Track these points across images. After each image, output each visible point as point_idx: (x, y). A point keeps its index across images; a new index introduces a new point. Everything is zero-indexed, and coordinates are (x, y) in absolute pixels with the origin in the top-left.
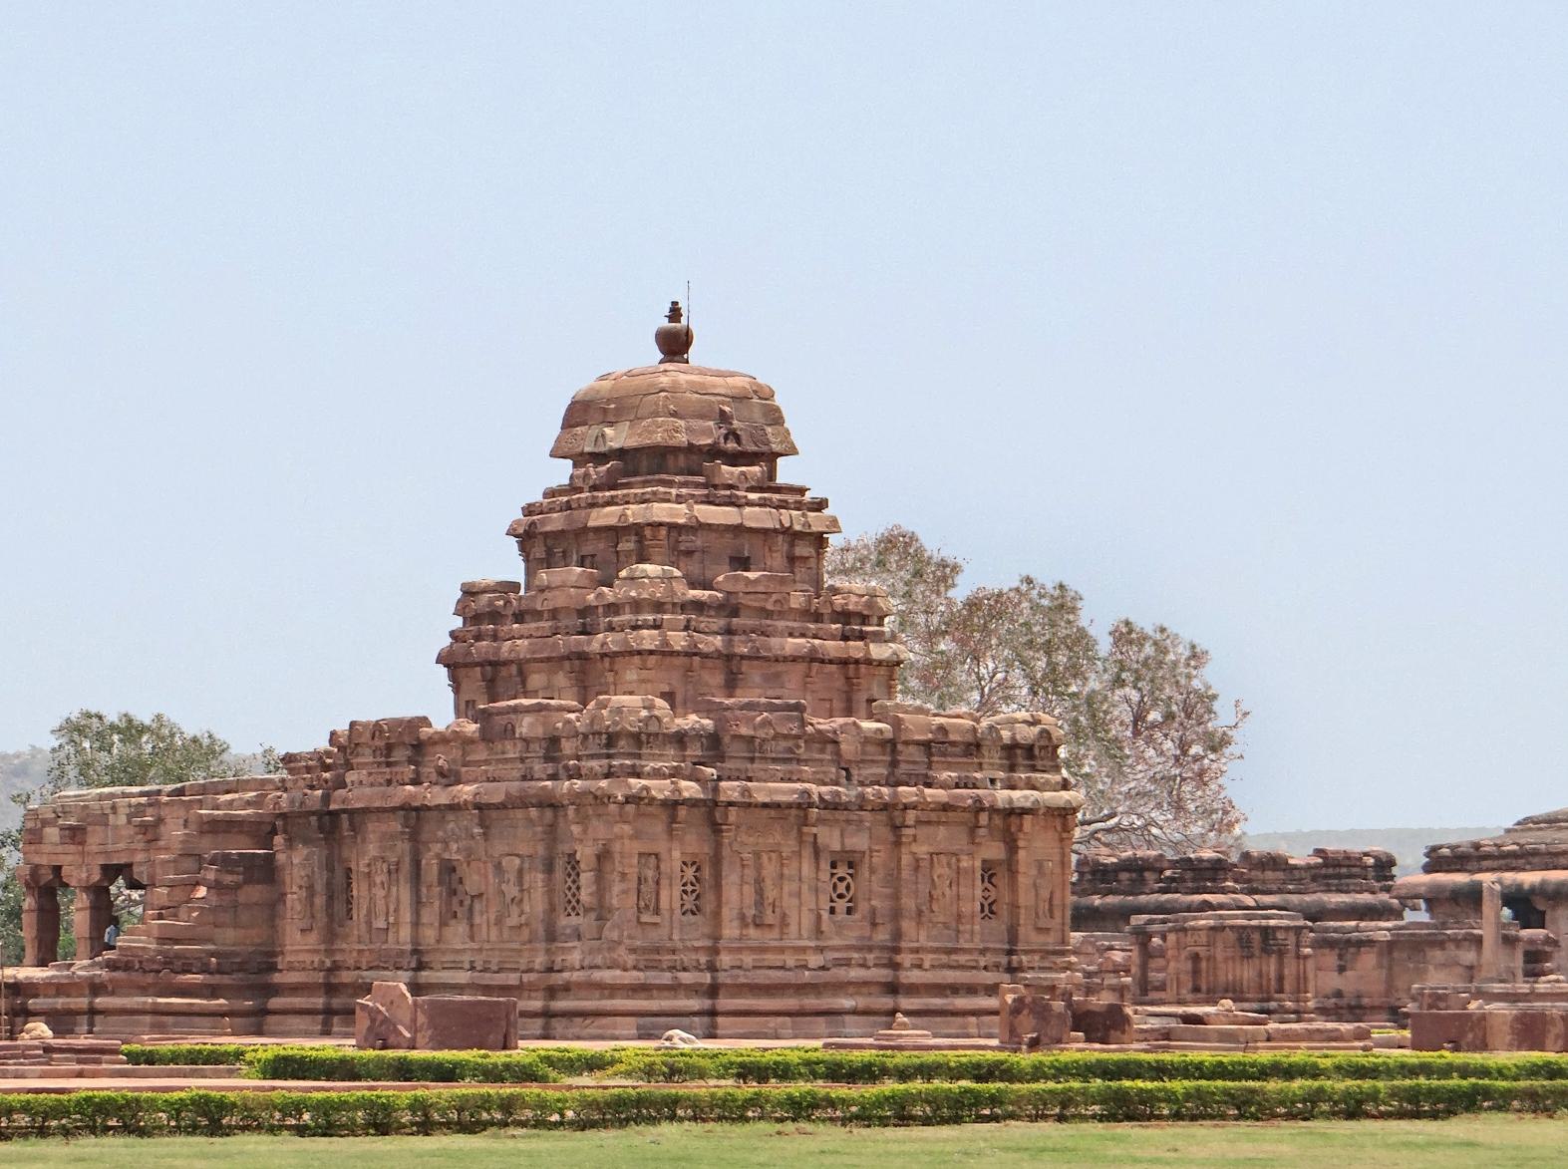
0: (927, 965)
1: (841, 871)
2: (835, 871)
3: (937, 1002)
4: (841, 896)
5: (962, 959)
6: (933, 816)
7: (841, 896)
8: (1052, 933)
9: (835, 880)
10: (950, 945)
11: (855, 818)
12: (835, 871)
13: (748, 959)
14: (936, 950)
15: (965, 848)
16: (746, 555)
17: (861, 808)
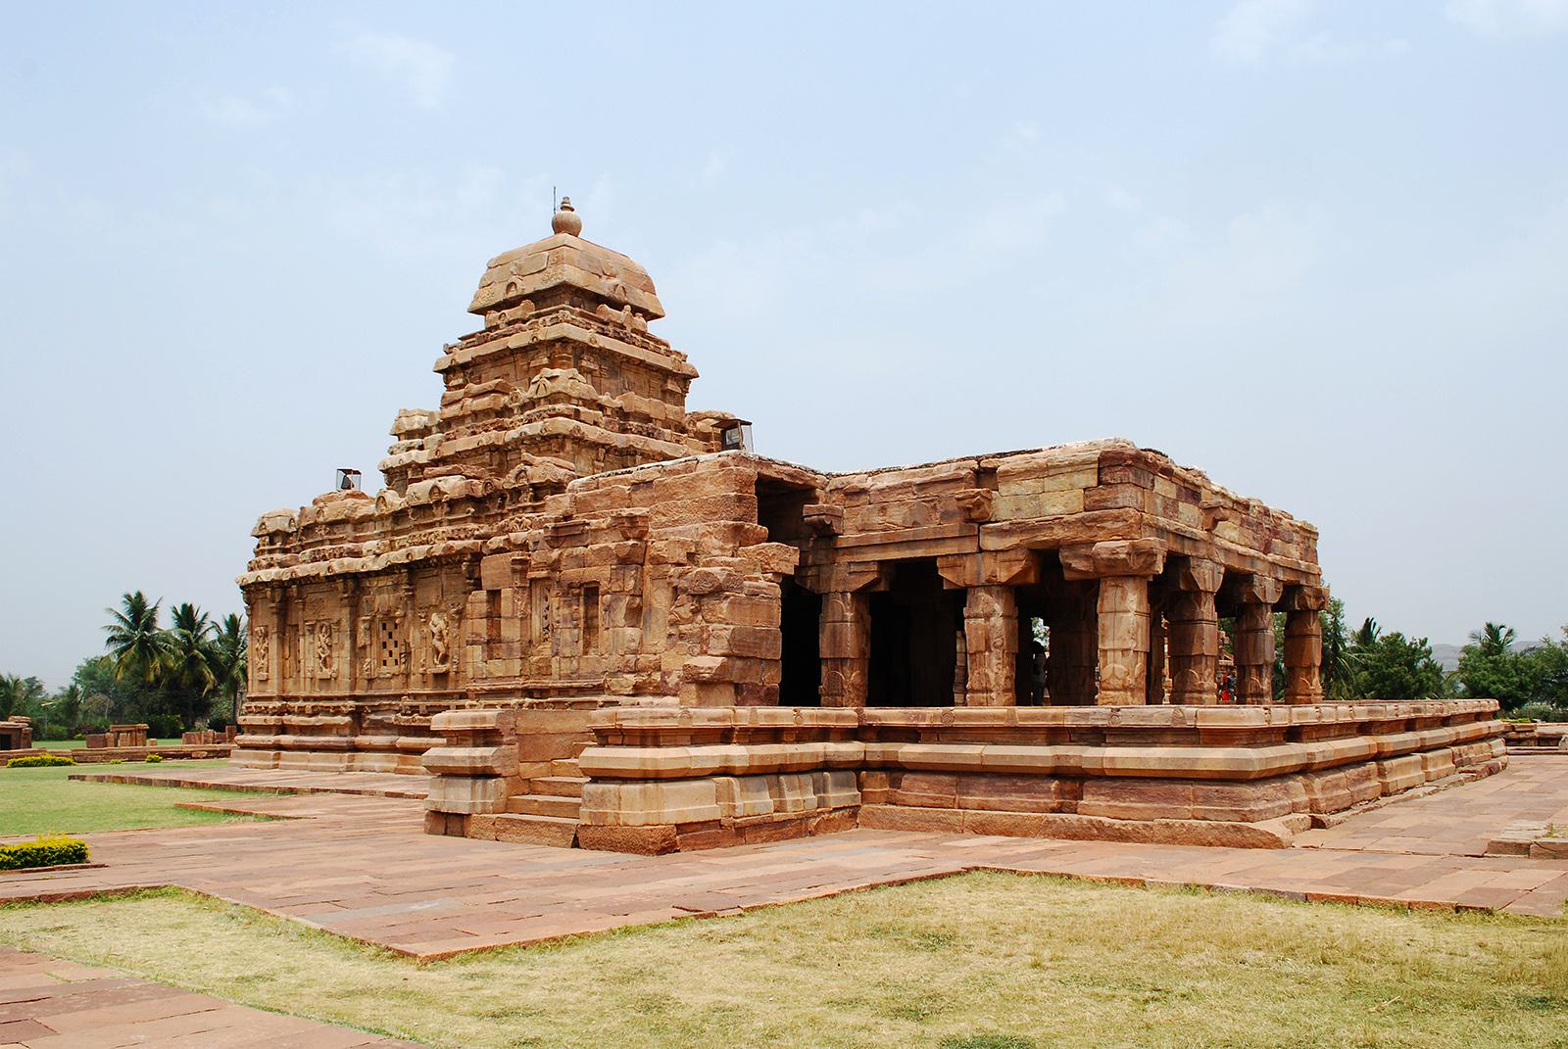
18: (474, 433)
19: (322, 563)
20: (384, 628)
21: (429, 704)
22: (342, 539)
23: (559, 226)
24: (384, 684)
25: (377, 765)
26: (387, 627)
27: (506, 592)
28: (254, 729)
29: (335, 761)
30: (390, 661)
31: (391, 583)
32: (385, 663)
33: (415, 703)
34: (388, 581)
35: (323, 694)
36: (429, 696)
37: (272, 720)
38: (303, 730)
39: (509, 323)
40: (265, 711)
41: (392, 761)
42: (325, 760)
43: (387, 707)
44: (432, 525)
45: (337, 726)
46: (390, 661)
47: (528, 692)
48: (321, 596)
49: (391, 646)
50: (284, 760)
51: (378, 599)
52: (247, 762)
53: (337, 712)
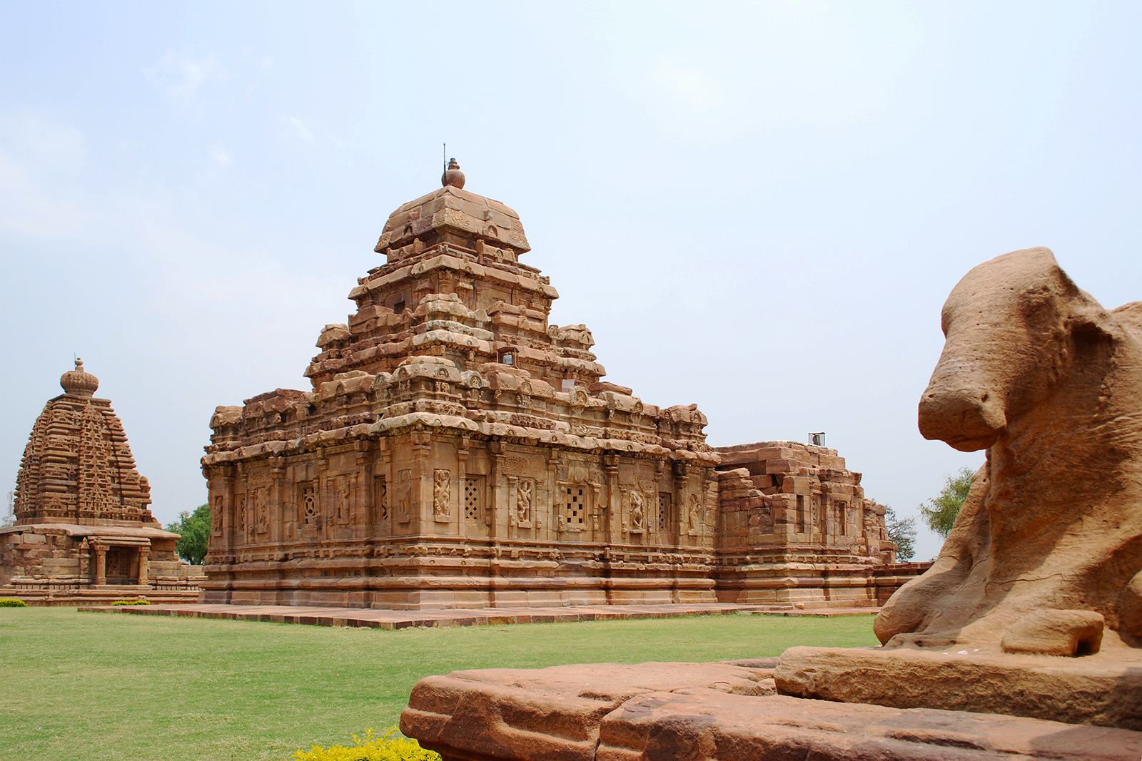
0: (331, 555)
1: (309, 495)
2: (306, 495)
3: (330, 581)
4: (311, 511)
5: (349, 549)
6: (338, 449)
7: (311, 511)
8: (410, 526)
9: (306, 501)
10: (346, 540)
11: (306, 458)
12: (306, 495)
13: (250, 555)
14: (339, 544)
15: (355, 468)
16: (403, 300)
17: (306, 451)
18: (531, 347)
19: (624, 442)
20: (569, 492)
21: (632, 554)
22: (542, 413)
23: (446, 181)
24: (573, 536)
25: (585, 600)
26: (572, 492)
27: (806, 498)
28: (435, 570)
29: (556, 598)
30: (575, 519)
31: (582, 460)
32: (569, 520)
33: (622, 553)
34: (581, 457)
35: (523, 541)
36: (629, 548)
37: (472, 562)
38: (505, 572)
39: (505, 262)
40: (461, 553)
41: (666, 596)
42: (543, 597)
43: (580, 555)
44: (629, 428)
45: (547, 571)
46: (575, 519)
47: (815, 551)
48: (522, 456)
49: (575, 507)
50: (498, 599)
51: (571, 470)
52: (449, 603)
53: (547, 557)
